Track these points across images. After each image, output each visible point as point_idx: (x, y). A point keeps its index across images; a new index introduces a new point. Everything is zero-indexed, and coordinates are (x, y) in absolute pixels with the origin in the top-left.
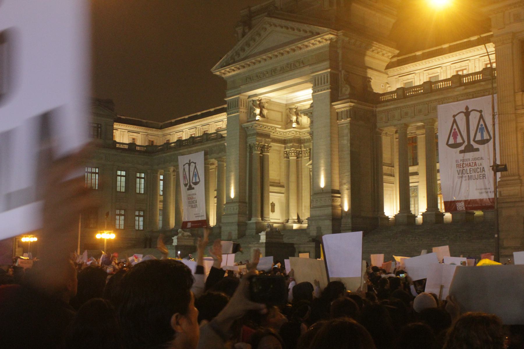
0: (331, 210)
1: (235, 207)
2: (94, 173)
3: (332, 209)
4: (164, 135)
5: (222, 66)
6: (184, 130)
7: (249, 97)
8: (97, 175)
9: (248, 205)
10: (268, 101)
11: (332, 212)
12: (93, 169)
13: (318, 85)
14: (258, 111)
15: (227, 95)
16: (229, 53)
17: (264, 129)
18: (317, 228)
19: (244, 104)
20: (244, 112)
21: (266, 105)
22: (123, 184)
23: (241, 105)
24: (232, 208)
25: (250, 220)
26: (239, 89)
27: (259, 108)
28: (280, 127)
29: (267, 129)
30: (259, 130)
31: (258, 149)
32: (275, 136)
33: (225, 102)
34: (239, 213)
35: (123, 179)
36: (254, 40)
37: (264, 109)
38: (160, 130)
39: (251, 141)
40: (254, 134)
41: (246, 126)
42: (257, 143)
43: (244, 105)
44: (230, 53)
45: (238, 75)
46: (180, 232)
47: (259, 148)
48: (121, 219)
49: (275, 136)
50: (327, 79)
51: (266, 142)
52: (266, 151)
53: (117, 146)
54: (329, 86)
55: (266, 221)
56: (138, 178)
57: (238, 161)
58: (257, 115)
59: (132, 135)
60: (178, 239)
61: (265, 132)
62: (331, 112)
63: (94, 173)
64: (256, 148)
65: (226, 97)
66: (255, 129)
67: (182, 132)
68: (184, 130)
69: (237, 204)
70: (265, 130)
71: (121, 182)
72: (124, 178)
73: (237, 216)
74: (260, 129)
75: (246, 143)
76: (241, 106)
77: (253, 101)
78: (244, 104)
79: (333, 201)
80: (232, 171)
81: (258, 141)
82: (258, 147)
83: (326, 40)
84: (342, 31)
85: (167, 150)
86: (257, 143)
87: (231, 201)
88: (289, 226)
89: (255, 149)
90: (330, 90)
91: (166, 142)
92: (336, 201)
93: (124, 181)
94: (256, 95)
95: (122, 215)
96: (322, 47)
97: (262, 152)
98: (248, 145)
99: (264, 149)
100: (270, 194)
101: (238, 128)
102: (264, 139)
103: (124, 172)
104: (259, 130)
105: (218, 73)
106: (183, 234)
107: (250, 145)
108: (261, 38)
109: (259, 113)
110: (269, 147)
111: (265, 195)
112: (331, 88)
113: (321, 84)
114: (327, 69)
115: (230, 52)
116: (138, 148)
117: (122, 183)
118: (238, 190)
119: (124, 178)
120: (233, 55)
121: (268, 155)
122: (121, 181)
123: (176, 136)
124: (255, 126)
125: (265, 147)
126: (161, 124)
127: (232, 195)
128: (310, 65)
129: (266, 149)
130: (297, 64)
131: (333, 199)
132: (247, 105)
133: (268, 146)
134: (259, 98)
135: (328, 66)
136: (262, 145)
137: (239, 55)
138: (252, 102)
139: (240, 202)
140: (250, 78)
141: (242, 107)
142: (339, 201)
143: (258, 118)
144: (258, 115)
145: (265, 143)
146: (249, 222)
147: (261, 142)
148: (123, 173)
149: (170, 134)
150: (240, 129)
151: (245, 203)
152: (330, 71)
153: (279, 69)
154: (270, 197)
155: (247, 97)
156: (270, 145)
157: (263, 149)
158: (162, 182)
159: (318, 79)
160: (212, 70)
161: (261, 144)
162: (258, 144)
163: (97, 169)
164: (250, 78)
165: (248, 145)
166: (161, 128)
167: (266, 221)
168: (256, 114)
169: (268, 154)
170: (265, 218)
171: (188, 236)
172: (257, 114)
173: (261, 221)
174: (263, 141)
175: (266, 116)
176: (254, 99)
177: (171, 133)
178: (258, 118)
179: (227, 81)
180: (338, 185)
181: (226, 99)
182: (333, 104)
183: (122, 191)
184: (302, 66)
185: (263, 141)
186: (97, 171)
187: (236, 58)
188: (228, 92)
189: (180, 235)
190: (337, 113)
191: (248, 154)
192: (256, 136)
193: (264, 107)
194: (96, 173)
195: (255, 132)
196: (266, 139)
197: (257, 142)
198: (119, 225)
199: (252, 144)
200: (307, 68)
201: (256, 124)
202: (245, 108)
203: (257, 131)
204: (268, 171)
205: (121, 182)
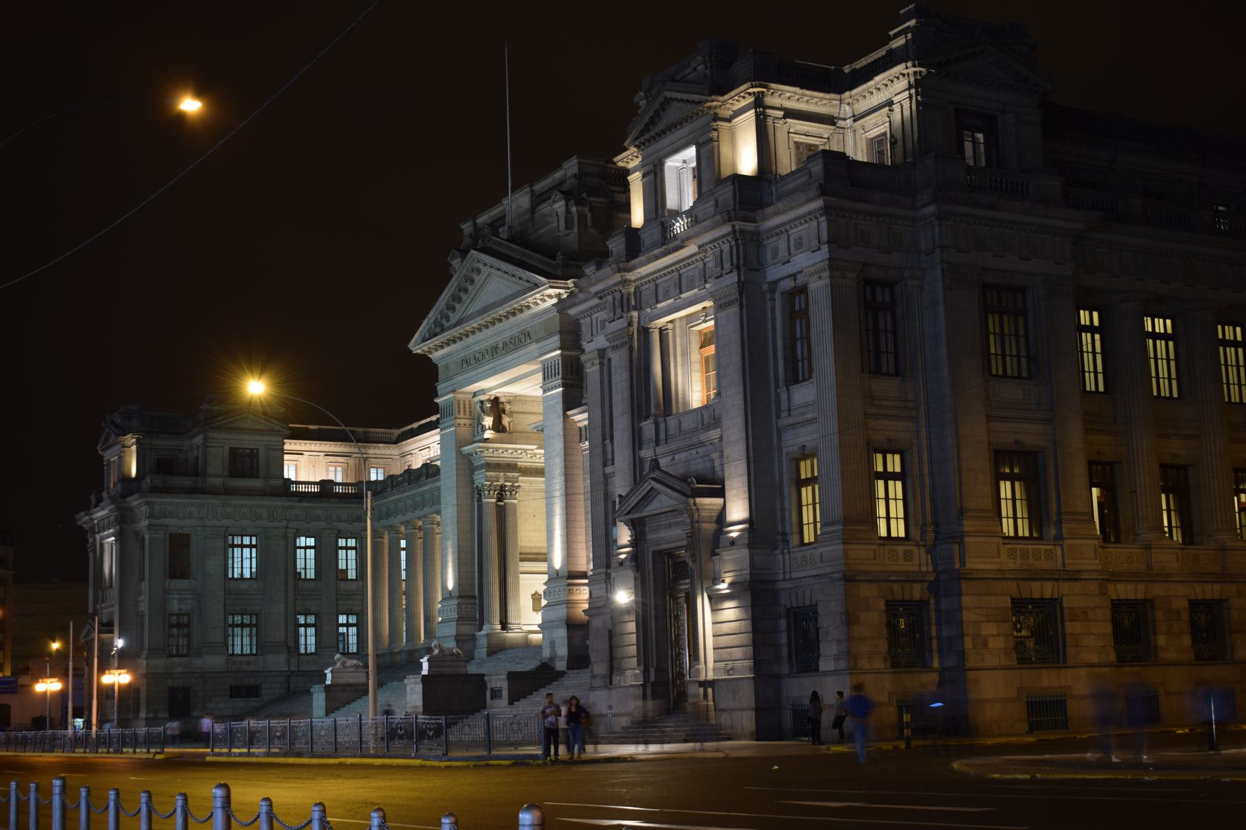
0: (565, 610)
1: (453, 607)
2: (246, 546)
3: (567, 607)
4: (403, 455)
5: (424, 340)
6: (431, 445)
7: (475, 394)
8: (254, 550)
9: (477, 601)
10: (511, 398)
11: (567, 613)
12: (244, 538)
13: (555, 376)
14: (488, 421)
15: (439, 393)
16: (430, 315)
17: (501, 455)
18: (550, 642)
19: (465, 408)
20: (465, 425)
21: (508, 407)
22: (311, 564)
23: (459, 411)
24: (449, 608)
25: (480, 629)
26: (453, 382)
27: (490, 416)
28: (535, 447)
29: (506, 455)
30: (492, 457)
31: (489, 493)
32: (535, 463)
33: (435, 409)
34: (459, 619)
35: (311, 553)
36: (466, 291)
37: (503, 416)
38: (394, 446)
39: (481, 478)
40: (482, 466)
41: (467, 452)
42: (489, 483)
43: (465, 411)
44: (432, 315)
45: (450, 354)
46: (338, 659)
47: (492, 492)
48: (308, 633)
49: (535, 463)
50: (558, 368)
51: (509, 479)
52: (508, 496)
53: (293, 488)
54: (560, 381)
55: (512, 629)
56: (342, 548)
57: (456, 519)
58: (486, 430)
59: (333, 460)
60: (331, 672)
61: (506, 459)
62: (565, 428)
63: (246, 546)
64: (486, 492)
65: (437, 396)
66: (482, 457)
67: (428, 449)
68: (431, 445)
69: (455, 602)
70: (504, 456)
71: (306, 561)
72: (313, 551)
73: (455, 623)
74: (492, 455)
75: (473, 482)
76: (459, 414)
77: (482, 402)
78: (465, 408)
79: (570, 592)
80: (448, 538)
81: (488, 479)
82: (489, 491)
83: (550, 296)
84: (572, 280)
85: (392, 490)
86: (489, 483)
87: (448, 596)
88: (511, 638)
89: (485, 495)
90: (561, 389)
91: (406, 468)
92: (578, 592)
93: (313, 557)
94: (483, 392)
95: (311, 625)
96: (546, 311)
97: (500, 499)
98: (475, 486)
99: (505, 492)
100: (521, 575)
101: (454, 455)
102: (502, 474)
103: (313, 539)
104: (492, 457)
105: (419, 351)
106: (343, 664)
107: (477, 486)
108: (475, 286)
109: (491, 426)
110: (514, 489)
111: (510, 579)
112: (564, 385)
113: (555, 376)
114: (555, 350)
115: (432, 313)
116: (339, 489)
117: (308, 561)
118: (457, 573)
119: (313, 551)
120: (437, 318)
121: (514, 505)
122: (305, 559)
123: (420, 456)
124: (481, 451)
125: (506, 488)
126: (396, 433)
127: (450, 585)
128: (537, 341)
129: (508, 493)
130: (523, 339)
131: (570, 590)
132: (473, 411)
133: (512, 486)
134: (491, 395)
135: (558, 344)
136: (498, 485)
137: (448, 318)
138: (478, 405)
139: (460, 597)
140: (467, 362)
141: (462, 416)
142: (585, 592)
143: (488, 434)
144: (489, 429)
145: (506, 481)
146: (479, 633)
147: (498, 481)
148: (311, 541)
149: (411, 454)
150: (457, 458)
151: (474, 597)
152: (561, 354)
153: (501, 345)
154: (521, 581)
155: (472, 396)
156: (516, 484)
157: (502, 493)
158: (403, 554)
159: (551, 366)
160: (410, 346)
161: (495, 483)
162: (490, 485)
163: (254, 539)
164: (467, 362)
165: (475, 486)
166: (396, 442)
167: (512, 629)
168: (483, 427)
169: (516, 501)
170: (511, 624)
171: (356, 666)
172: (487, 427)
173: (499, 631)
174: (501, 478)
175: (508, 429)
176: (482, 398)
177: (413, 452)
178: (488, 434)
179: (439, 365)
180: (586, 563)
181: (437, 401)
182: (569, 413)
183: (308, 577)
184: (529, 341)
185: (501, 478)
186: (254, 542)
187: (446, 325)
188: (440, 387)
189: (338, 665)
190: (580, 429)
191: (476, 504)
192: (484, 470)
193: (504, 411)
194: (251, 546)
195: (484, 462)
196: (508, 474)
197: (487, 481)
198: (306, 644)
199: (480, 485)
200: (534, 346)
201: (480, 448)
202: (467, 416)
203: (486, 460)
204: (516, 532)
205: (306, 561)
